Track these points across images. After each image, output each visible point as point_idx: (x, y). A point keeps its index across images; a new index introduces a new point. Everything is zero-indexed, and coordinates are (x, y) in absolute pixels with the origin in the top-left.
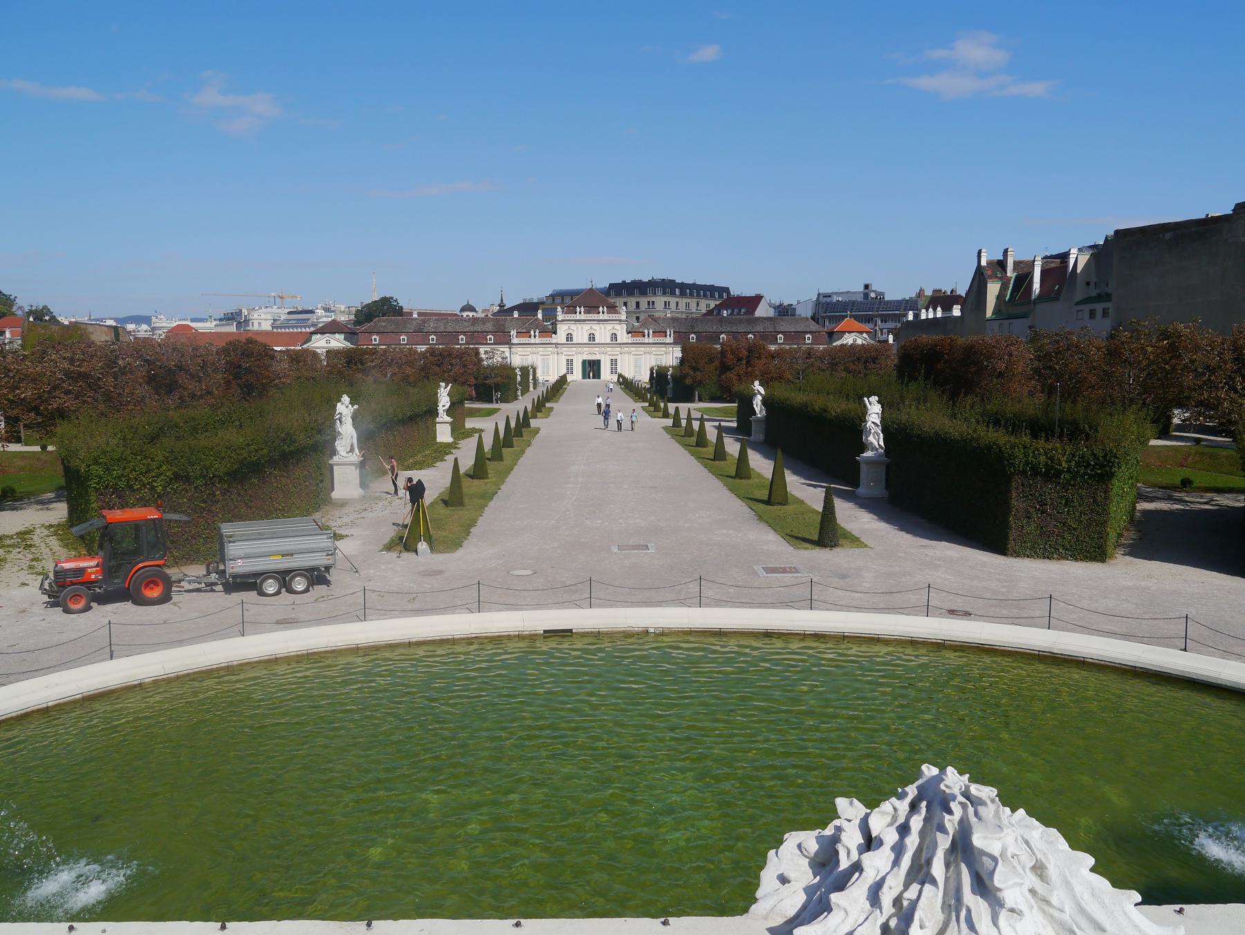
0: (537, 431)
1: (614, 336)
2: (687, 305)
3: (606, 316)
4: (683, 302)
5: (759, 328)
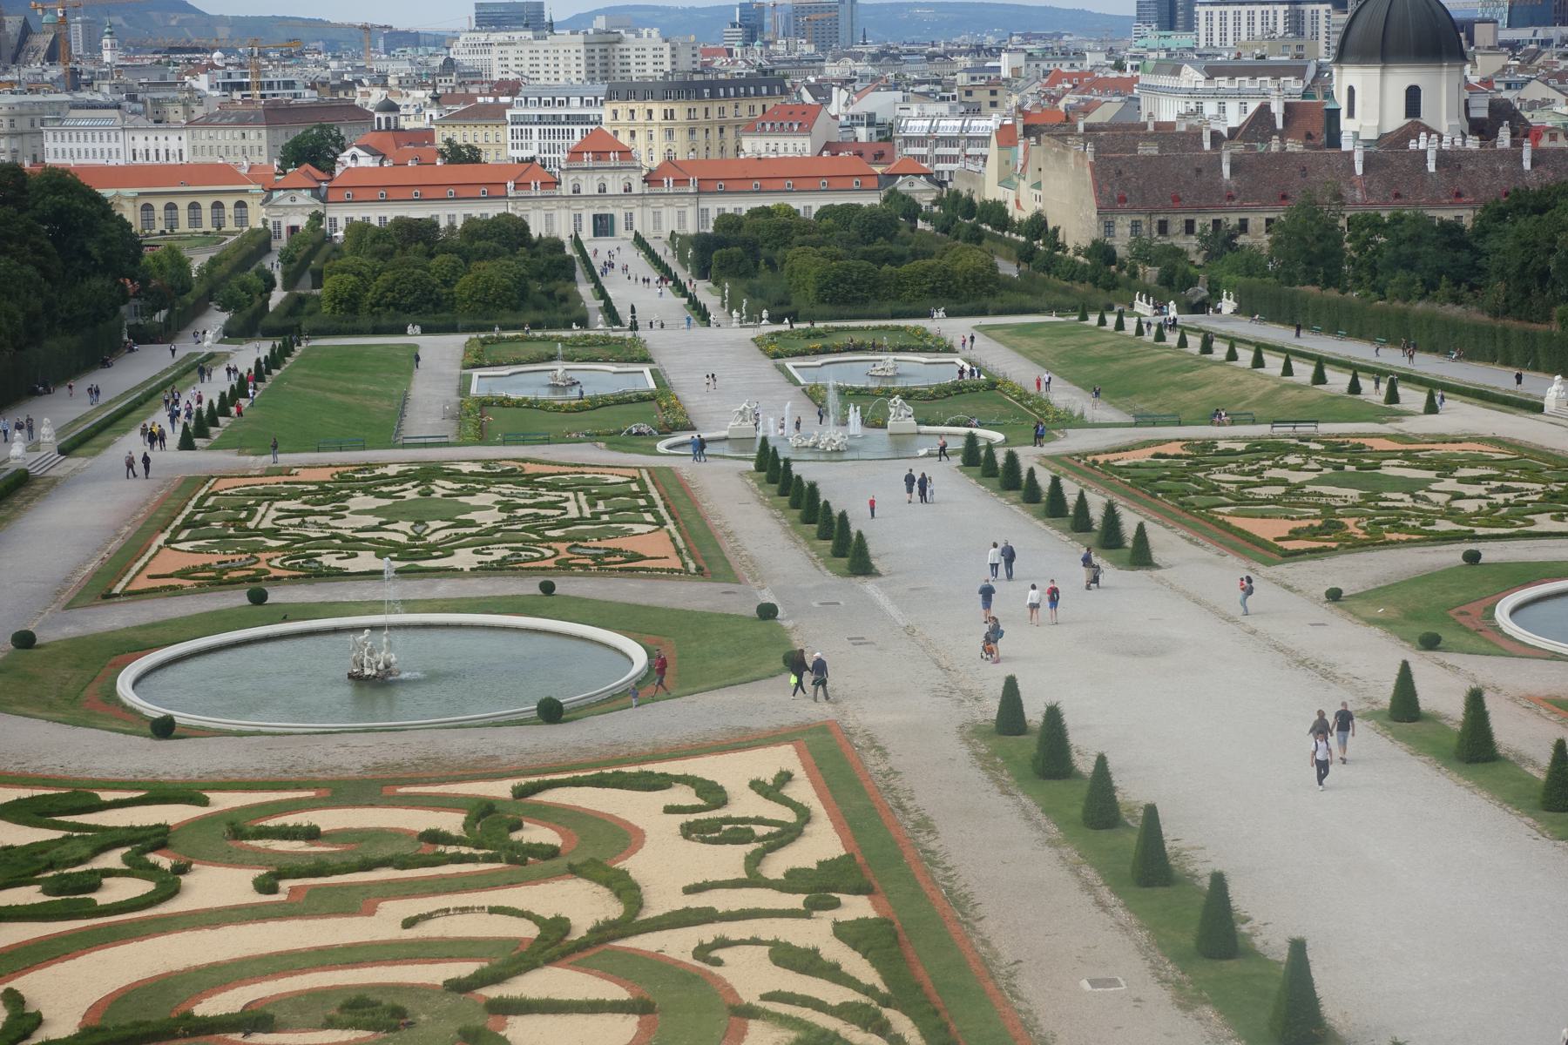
1: (628, 189)
4: (714, 108)
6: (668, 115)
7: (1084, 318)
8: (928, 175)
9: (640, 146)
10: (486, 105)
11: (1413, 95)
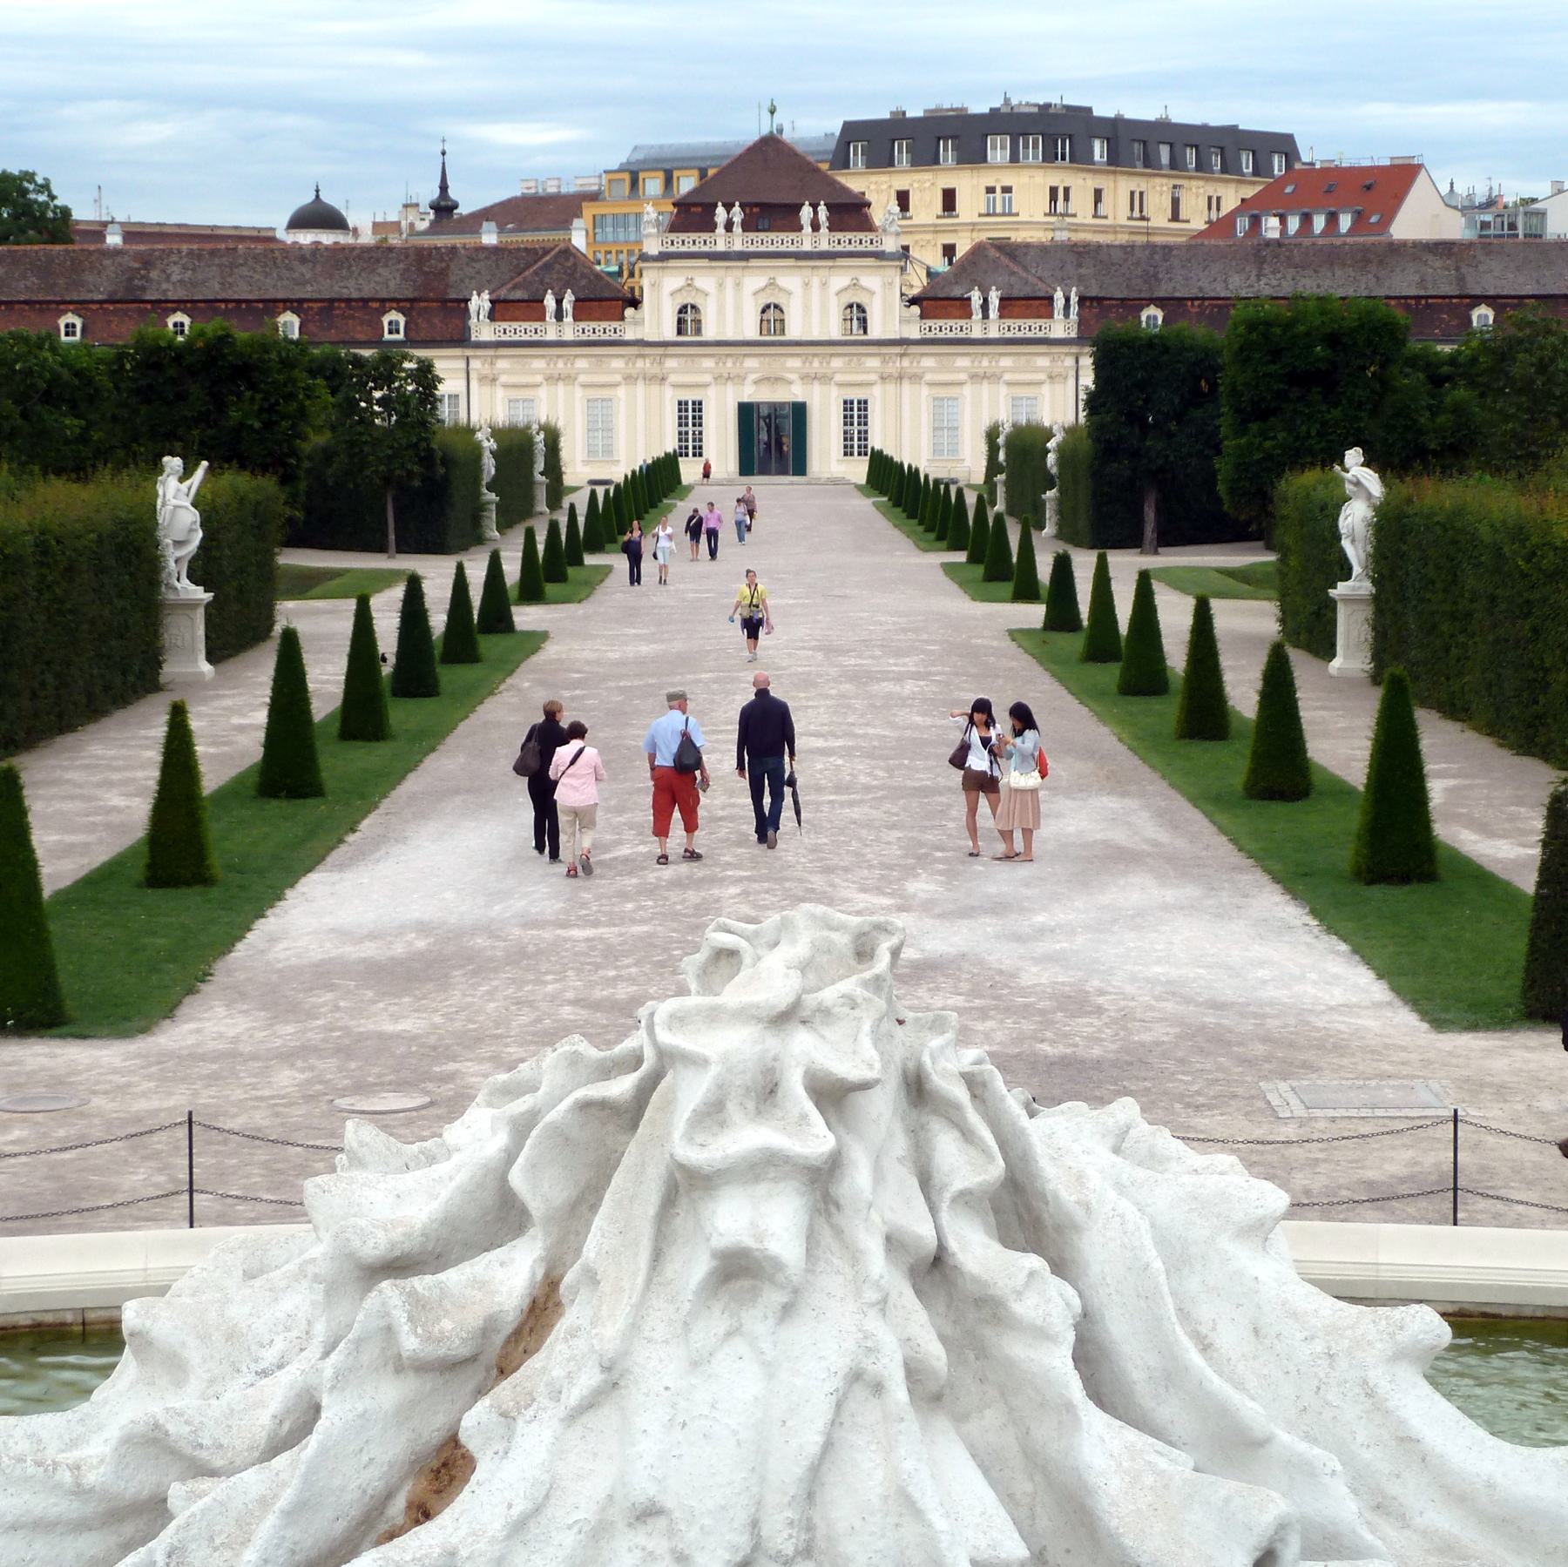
0: (537, 639)
1: (858, 314)
2: (1137, 201)
3: (825, 240)
4: (1119, 189)
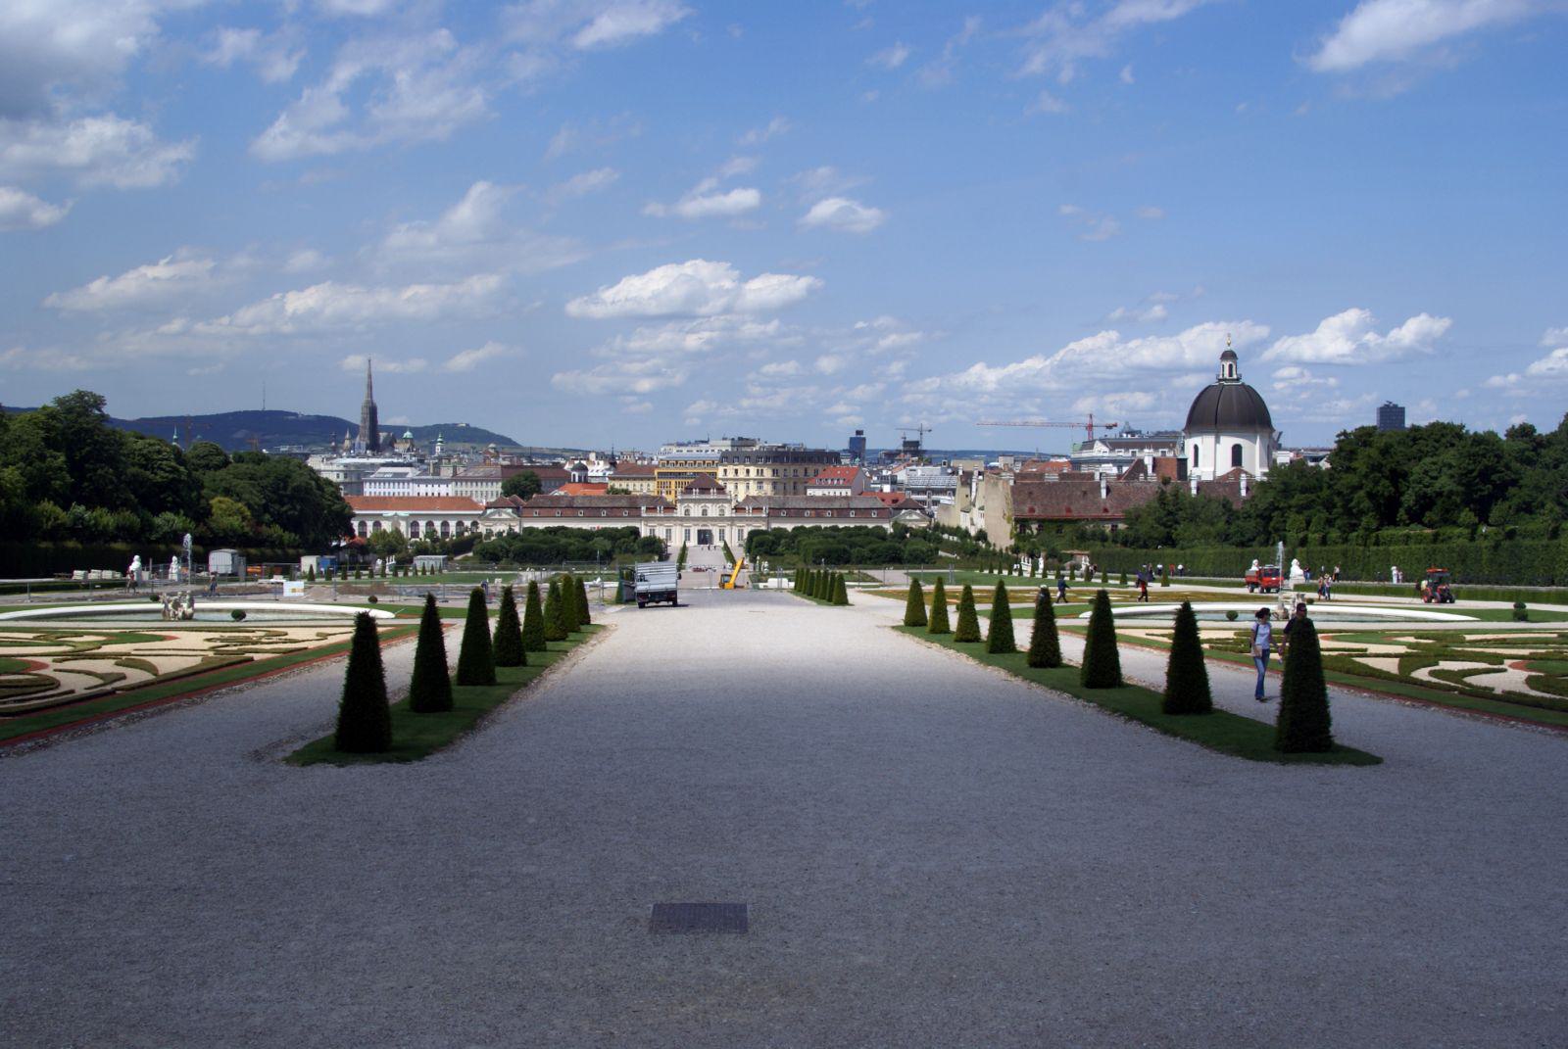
5: (837, 505)
6: (760, 472)
7: (982, 570)
8: (922, 509)
9: (730, 487)
10: (643, 466)
11: (1237, 451)
